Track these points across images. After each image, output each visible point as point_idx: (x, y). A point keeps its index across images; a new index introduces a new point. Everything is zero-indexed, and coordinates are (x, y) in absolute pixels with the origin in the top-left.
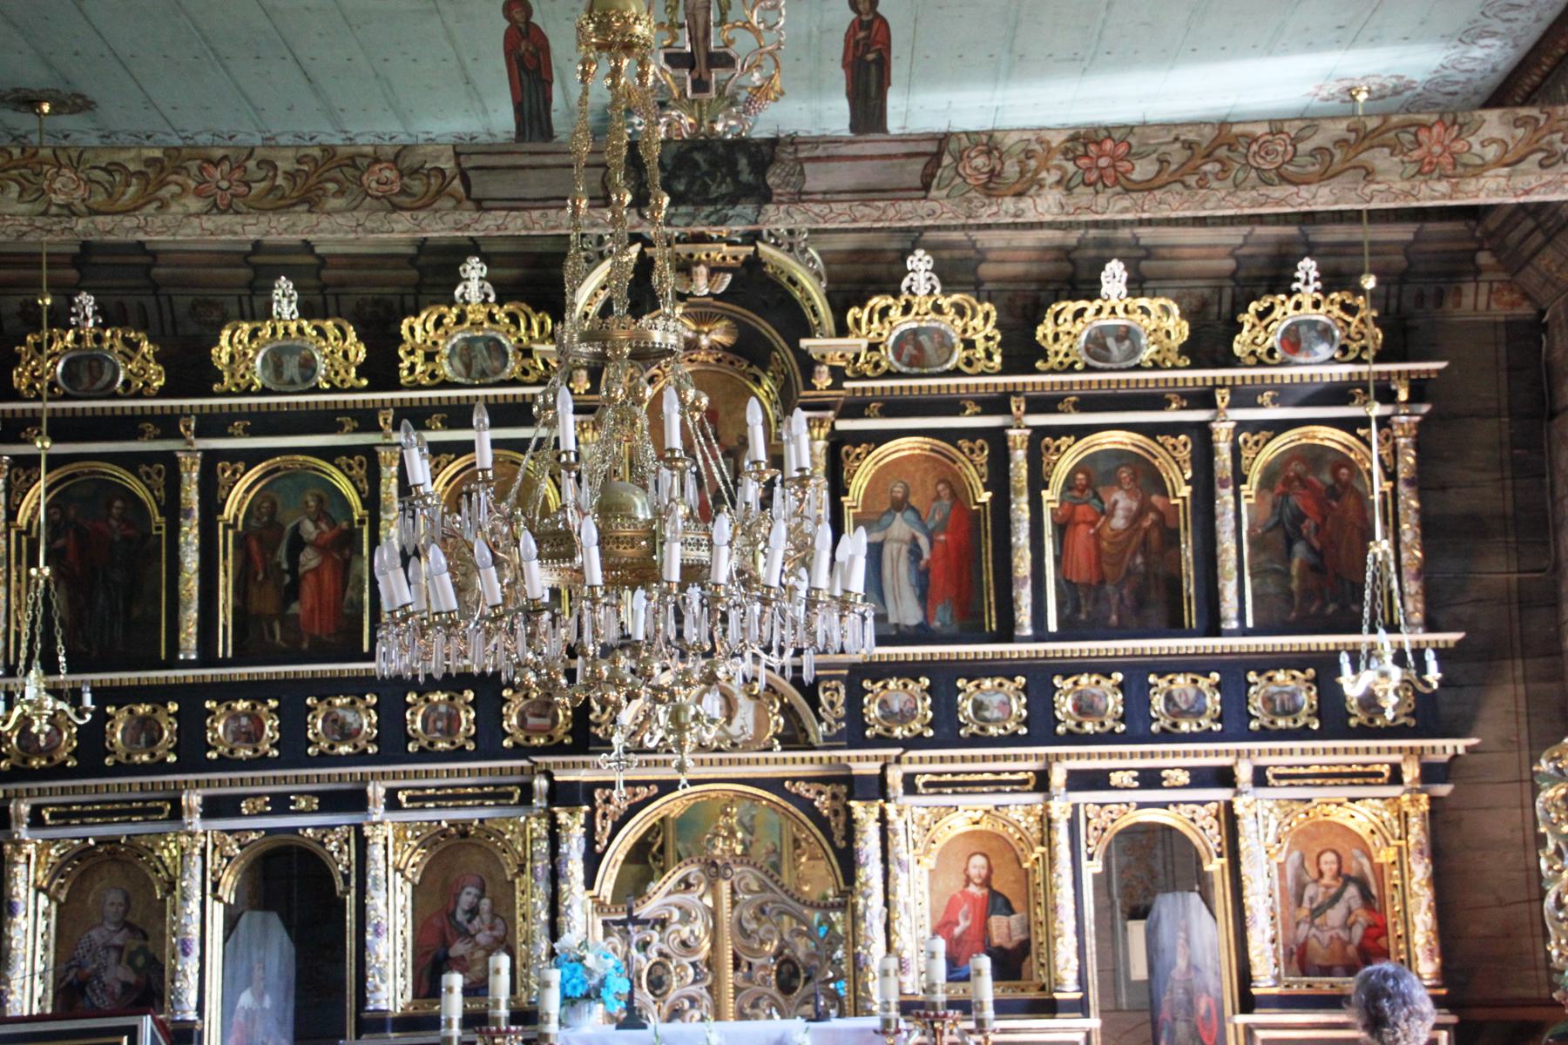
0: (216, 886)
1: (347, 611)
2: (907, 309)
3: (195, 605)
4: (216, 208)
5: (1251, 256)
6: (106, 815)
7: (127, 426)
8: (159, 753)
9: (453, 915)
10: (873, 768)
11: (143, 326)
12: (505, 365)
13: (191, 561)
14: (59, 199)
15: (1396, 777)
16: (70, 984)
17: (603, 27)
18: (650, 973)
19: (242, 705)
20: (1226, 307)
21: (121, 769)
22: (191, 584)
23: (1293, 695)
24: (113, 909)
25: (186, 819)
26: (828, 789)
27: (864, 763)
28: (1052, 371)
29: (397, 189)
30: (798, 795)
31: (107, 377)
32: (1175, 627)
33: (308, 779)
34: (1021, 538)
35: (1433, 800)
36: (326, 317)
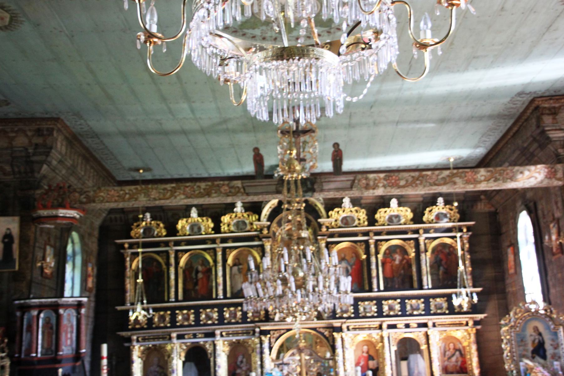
2: (344, 211)
4: (188, 197)
6: (154, 339)
7: (157, 244)
9: (236, 363)
10: (338, 325)
11: (160, 220)
13: (173, 277)
14: (153, 197)
15: (467, 324)
17: (290, 168)
19: (185, 312)
20: (421, 209)
21: (158, 328)
22: (173, 282)
23: (441, 304)
26: (328, 330)
27: (336, 323)
28: (379, 226)
29: (228, 191)
31: (152, 233)
32: (412, 288)
33: (201, 330)
34: (373, 267)
35: (477, 330)
36: (203, 216)
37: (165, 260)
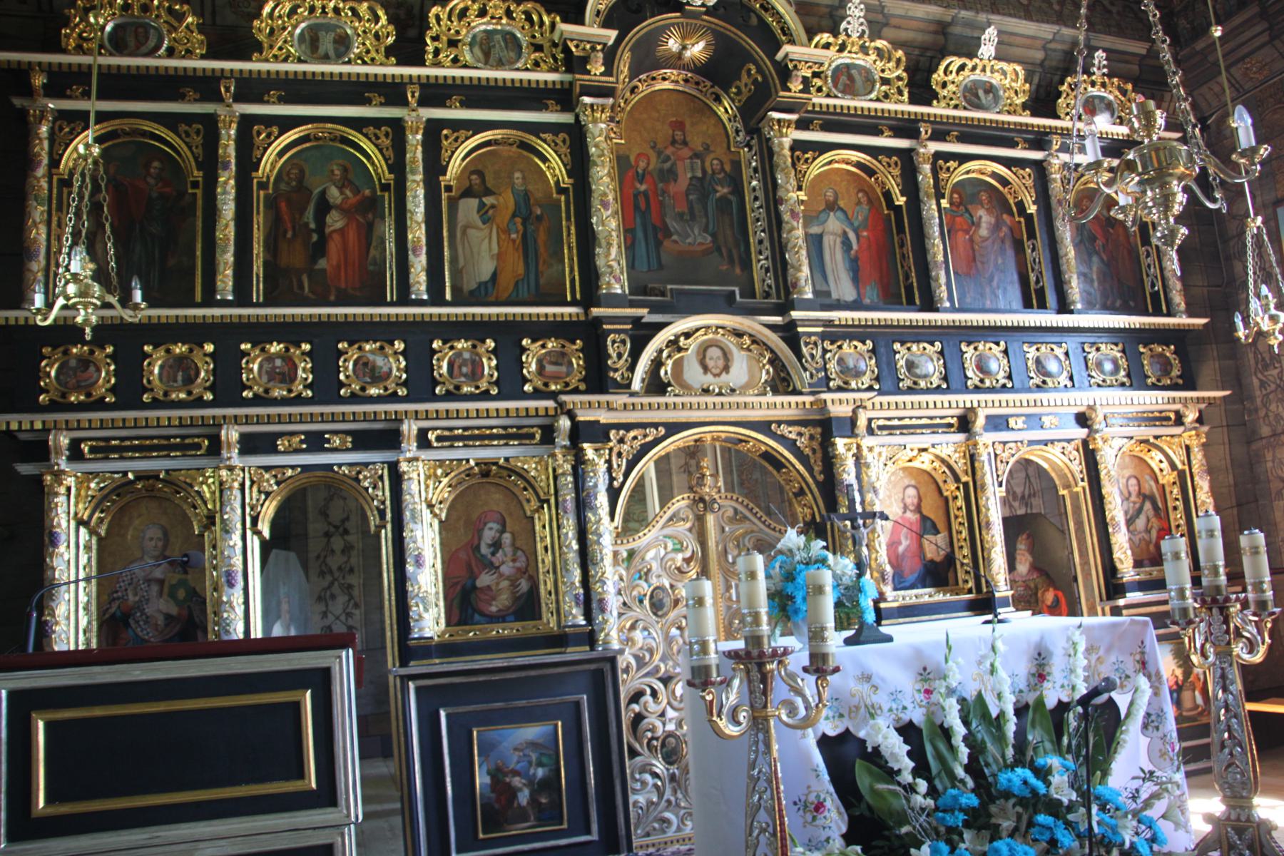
0: (255, 521)
1: (371, 268)
3: (232, 249)
5: (1055, 50)
6: (145, 450)
7: (170, 85)
9: (478, 547)
12: (519, 55)
13: (228, 209)
15: (1179, 420)
16: (113, 616)
18: (652, 597)
19: (275, 348)
21: (156, 404)
24: (153, 543)
25: (225, 454)
27: (839, 406)
30: (783, 436)
37: (199, 151)
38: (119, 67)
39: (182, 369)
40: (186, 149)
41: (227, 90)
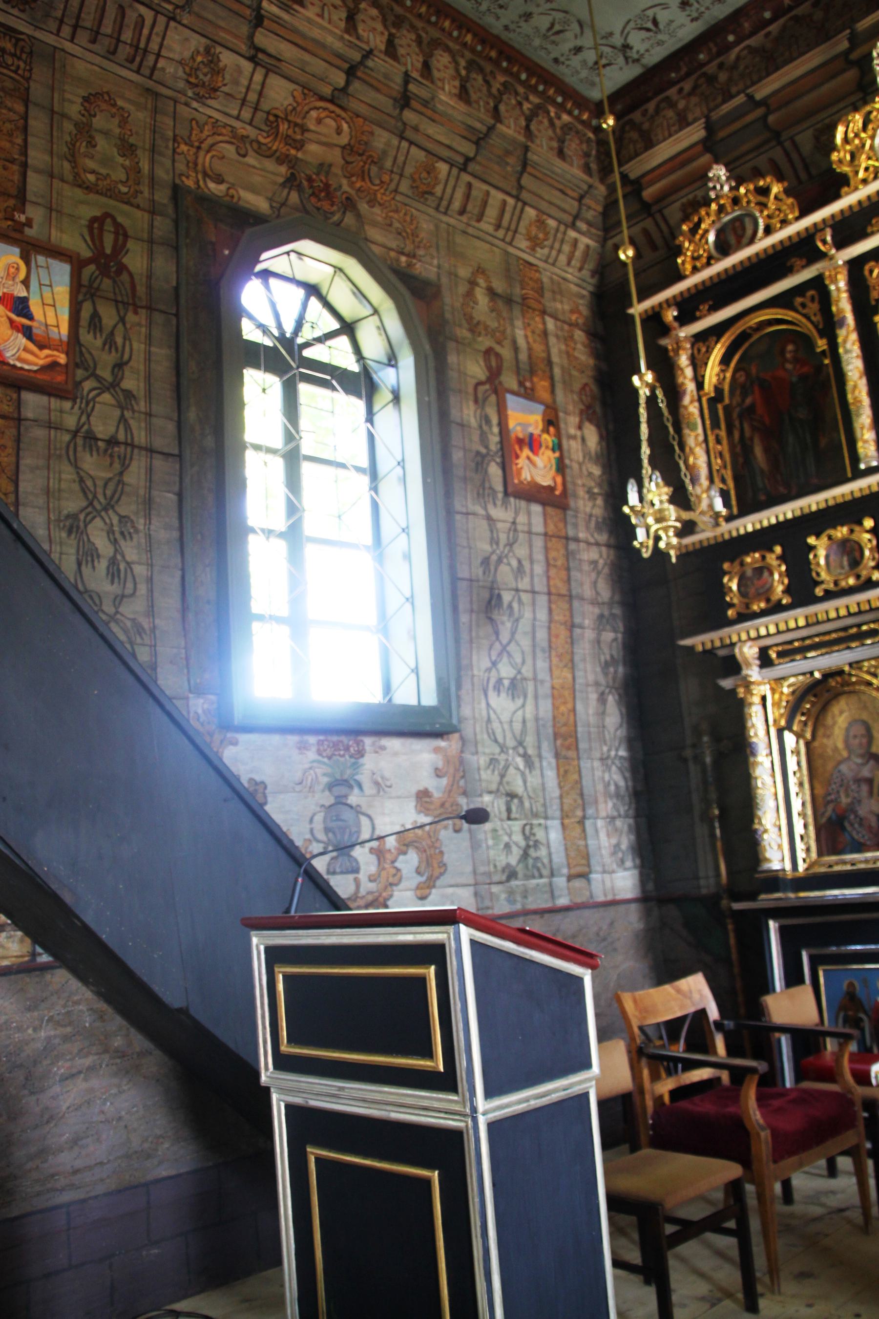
8: (864, 573)
21: (829, 595)
24: (857, 741)
38: (726, 270)
39: (851, 552)
40: (804, 320)
41: (824, 242)
